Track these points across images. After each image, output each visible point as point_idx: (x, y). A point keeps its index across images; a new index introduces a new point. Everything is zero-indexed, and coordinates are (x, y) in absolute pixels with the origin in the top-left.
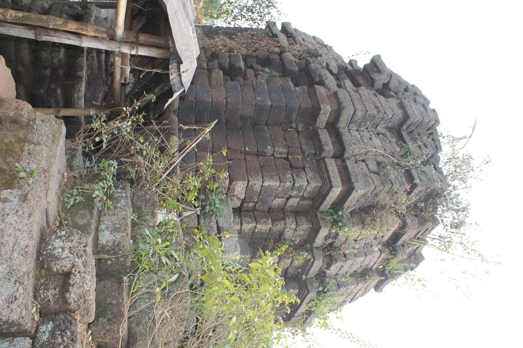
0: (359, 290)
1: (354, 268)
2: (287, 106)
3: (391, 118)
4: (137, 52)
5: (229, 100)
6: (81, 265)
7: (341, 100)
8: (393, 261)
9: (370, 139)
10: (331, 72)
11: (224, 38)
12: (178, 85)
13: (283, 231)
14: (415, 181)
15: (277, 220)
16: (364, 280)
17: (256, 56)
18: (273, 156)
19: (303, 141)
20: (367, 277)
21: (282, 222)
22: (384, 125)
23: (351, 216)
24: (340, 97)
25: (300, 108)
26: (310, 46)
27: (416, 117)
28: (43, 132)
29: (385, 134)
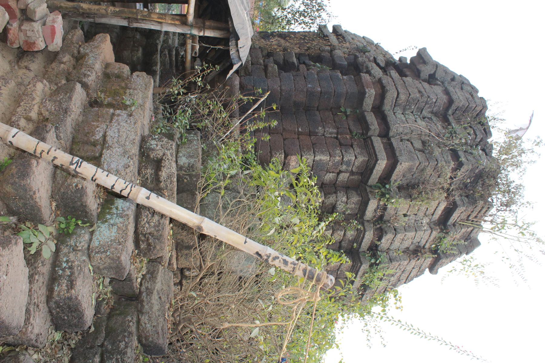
0: (413, 268)
1: (406, 244)
2: (335, 92)
3: (435, 103)
4: (204, 33)
5: (283, 88)
6: (169, 154)
7: (385, 85)
8: (445, 241)
9: (416, 121)
10: (378, 65)
11: (279, 39)
12: (237, 59)
13: (336, 204)
14: (460, 159)
15: (329, 194)
16: (416, 257)
17: (308, 55)
18: (324, 135)
19: (351, 123)
20: (419, 254)
21: (334, 195)
22: (429, 110)
23: (399, 191)
24: (383, 82)
25: (347, 93)
26: (358, 44)
27: (461, 101)
28: (138, 83)
29: (431, 118)
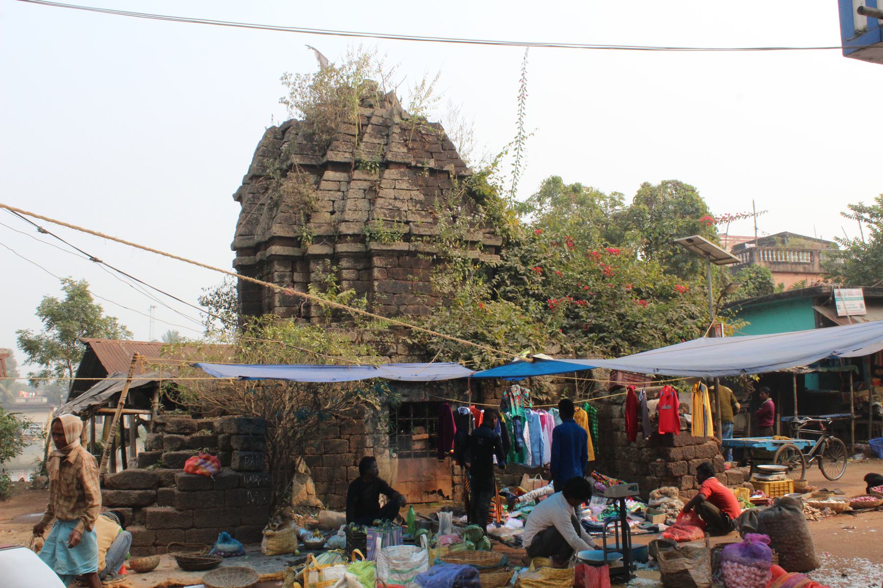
1: (363, 204)
